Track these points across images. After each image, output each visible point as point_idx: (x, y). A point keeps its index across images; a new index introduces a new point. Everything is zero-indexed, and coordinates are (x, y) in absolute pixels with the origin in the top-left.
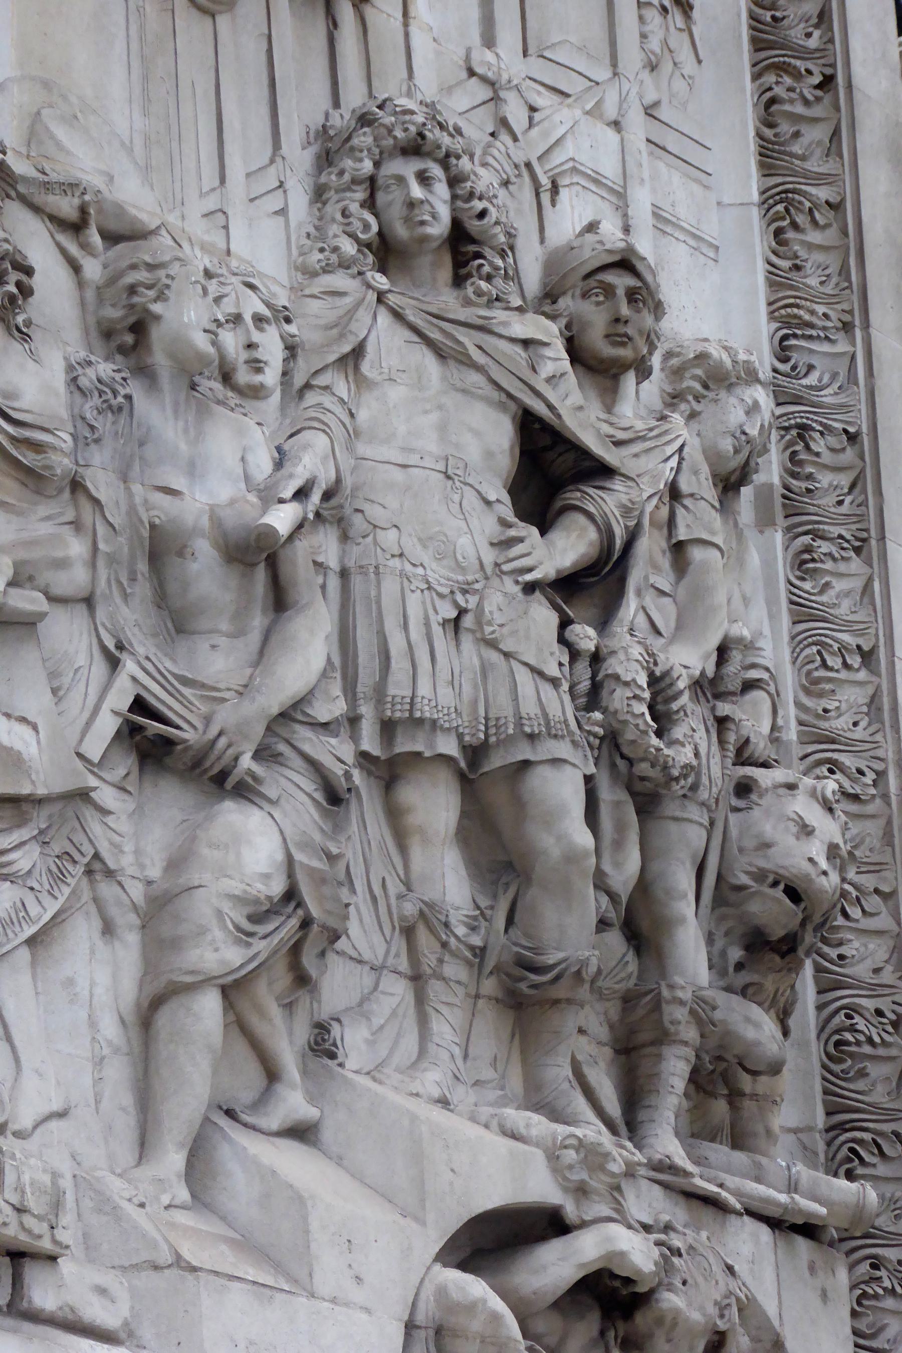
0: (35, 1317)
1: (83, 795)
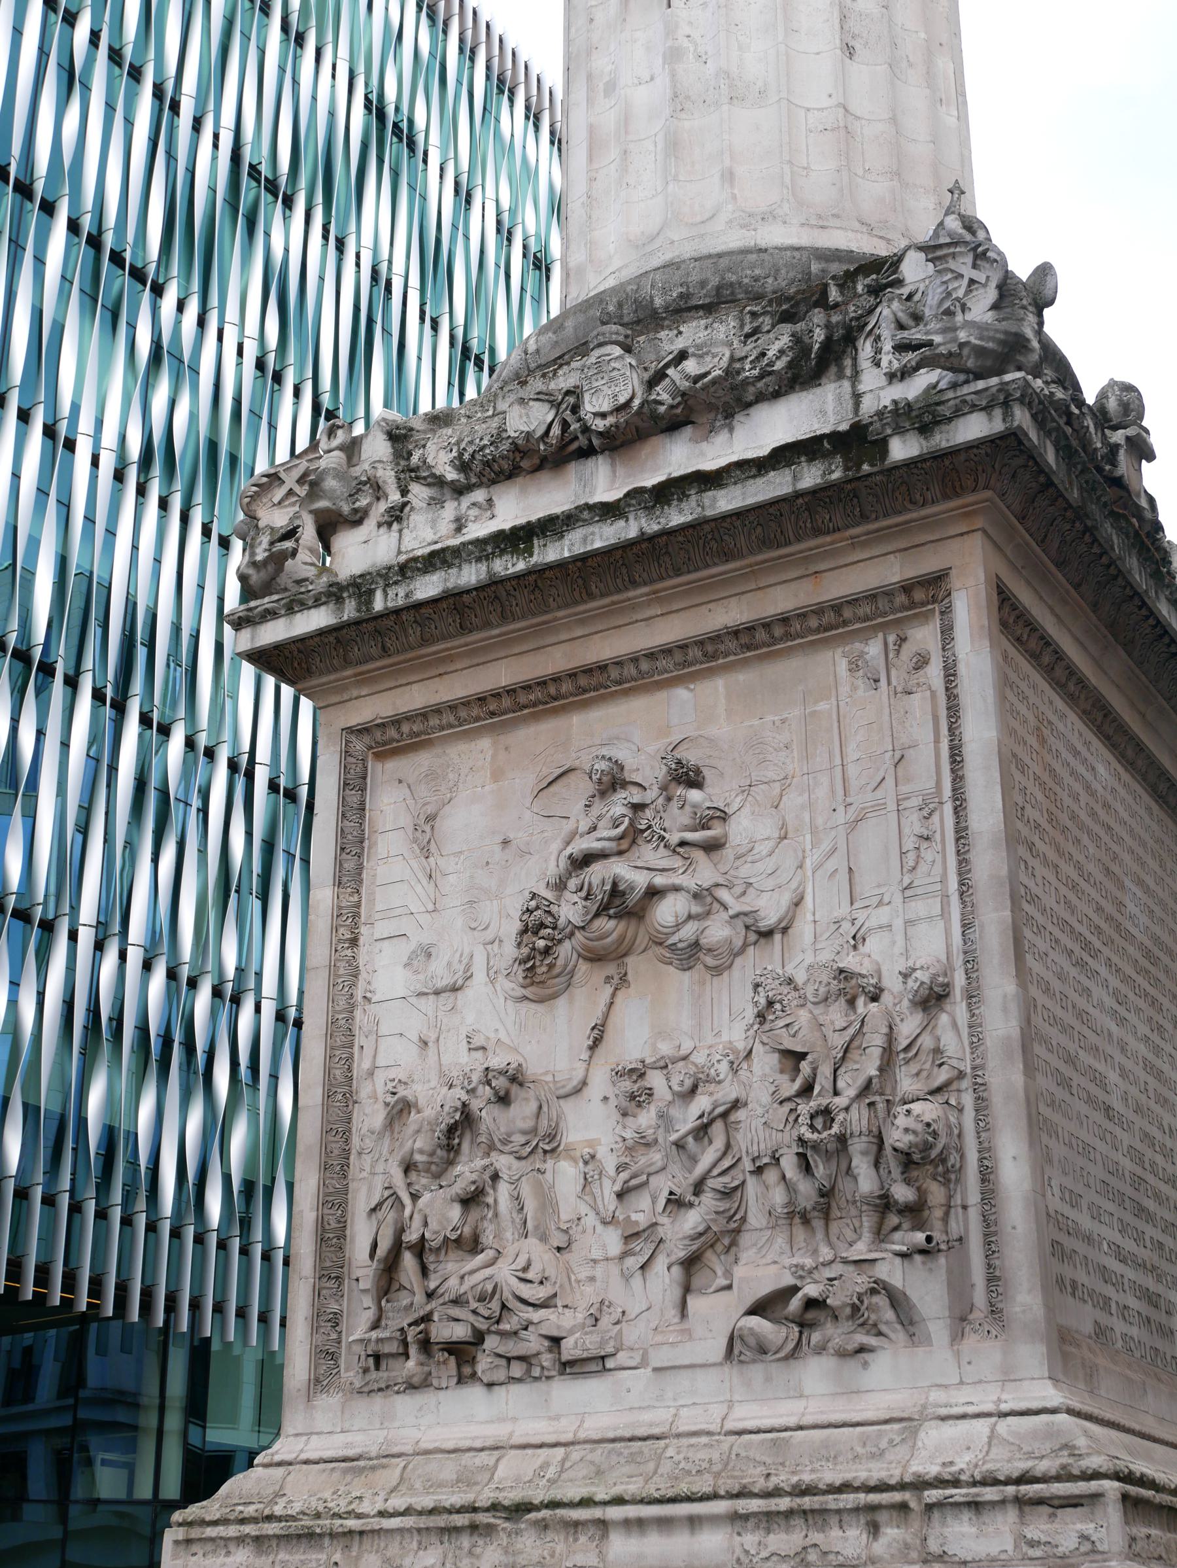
0: (610, 1370)
1: (656, 1224)
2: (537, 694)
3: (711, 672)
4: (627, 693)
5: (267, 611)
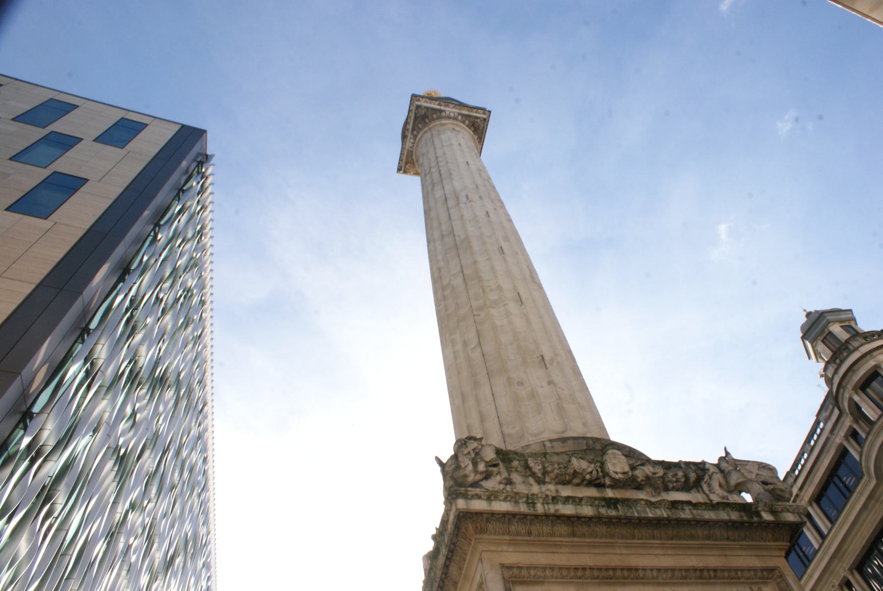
2: (603, 573)
3: (682, 584)
4: (644, 584)
5: (477, 495)
